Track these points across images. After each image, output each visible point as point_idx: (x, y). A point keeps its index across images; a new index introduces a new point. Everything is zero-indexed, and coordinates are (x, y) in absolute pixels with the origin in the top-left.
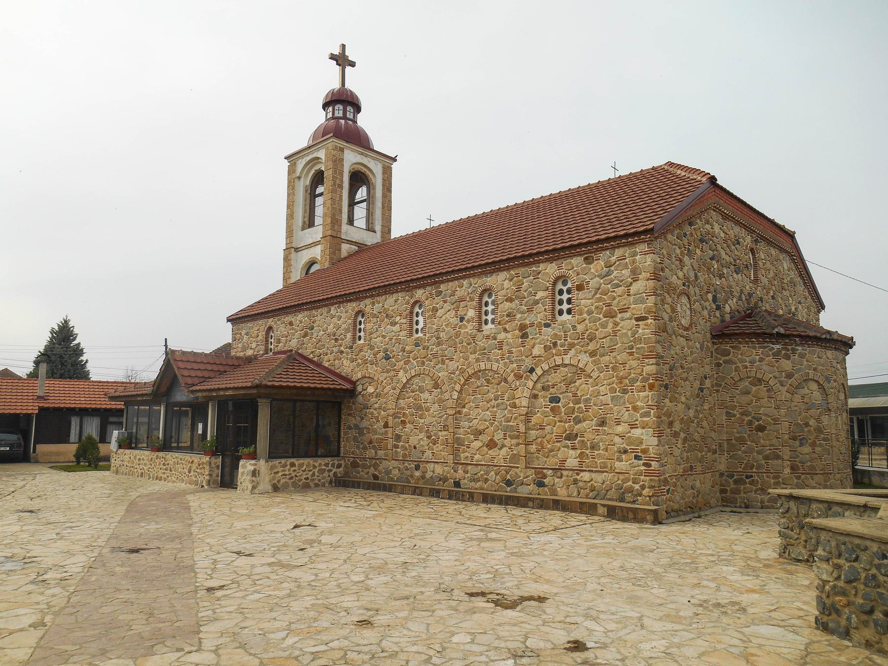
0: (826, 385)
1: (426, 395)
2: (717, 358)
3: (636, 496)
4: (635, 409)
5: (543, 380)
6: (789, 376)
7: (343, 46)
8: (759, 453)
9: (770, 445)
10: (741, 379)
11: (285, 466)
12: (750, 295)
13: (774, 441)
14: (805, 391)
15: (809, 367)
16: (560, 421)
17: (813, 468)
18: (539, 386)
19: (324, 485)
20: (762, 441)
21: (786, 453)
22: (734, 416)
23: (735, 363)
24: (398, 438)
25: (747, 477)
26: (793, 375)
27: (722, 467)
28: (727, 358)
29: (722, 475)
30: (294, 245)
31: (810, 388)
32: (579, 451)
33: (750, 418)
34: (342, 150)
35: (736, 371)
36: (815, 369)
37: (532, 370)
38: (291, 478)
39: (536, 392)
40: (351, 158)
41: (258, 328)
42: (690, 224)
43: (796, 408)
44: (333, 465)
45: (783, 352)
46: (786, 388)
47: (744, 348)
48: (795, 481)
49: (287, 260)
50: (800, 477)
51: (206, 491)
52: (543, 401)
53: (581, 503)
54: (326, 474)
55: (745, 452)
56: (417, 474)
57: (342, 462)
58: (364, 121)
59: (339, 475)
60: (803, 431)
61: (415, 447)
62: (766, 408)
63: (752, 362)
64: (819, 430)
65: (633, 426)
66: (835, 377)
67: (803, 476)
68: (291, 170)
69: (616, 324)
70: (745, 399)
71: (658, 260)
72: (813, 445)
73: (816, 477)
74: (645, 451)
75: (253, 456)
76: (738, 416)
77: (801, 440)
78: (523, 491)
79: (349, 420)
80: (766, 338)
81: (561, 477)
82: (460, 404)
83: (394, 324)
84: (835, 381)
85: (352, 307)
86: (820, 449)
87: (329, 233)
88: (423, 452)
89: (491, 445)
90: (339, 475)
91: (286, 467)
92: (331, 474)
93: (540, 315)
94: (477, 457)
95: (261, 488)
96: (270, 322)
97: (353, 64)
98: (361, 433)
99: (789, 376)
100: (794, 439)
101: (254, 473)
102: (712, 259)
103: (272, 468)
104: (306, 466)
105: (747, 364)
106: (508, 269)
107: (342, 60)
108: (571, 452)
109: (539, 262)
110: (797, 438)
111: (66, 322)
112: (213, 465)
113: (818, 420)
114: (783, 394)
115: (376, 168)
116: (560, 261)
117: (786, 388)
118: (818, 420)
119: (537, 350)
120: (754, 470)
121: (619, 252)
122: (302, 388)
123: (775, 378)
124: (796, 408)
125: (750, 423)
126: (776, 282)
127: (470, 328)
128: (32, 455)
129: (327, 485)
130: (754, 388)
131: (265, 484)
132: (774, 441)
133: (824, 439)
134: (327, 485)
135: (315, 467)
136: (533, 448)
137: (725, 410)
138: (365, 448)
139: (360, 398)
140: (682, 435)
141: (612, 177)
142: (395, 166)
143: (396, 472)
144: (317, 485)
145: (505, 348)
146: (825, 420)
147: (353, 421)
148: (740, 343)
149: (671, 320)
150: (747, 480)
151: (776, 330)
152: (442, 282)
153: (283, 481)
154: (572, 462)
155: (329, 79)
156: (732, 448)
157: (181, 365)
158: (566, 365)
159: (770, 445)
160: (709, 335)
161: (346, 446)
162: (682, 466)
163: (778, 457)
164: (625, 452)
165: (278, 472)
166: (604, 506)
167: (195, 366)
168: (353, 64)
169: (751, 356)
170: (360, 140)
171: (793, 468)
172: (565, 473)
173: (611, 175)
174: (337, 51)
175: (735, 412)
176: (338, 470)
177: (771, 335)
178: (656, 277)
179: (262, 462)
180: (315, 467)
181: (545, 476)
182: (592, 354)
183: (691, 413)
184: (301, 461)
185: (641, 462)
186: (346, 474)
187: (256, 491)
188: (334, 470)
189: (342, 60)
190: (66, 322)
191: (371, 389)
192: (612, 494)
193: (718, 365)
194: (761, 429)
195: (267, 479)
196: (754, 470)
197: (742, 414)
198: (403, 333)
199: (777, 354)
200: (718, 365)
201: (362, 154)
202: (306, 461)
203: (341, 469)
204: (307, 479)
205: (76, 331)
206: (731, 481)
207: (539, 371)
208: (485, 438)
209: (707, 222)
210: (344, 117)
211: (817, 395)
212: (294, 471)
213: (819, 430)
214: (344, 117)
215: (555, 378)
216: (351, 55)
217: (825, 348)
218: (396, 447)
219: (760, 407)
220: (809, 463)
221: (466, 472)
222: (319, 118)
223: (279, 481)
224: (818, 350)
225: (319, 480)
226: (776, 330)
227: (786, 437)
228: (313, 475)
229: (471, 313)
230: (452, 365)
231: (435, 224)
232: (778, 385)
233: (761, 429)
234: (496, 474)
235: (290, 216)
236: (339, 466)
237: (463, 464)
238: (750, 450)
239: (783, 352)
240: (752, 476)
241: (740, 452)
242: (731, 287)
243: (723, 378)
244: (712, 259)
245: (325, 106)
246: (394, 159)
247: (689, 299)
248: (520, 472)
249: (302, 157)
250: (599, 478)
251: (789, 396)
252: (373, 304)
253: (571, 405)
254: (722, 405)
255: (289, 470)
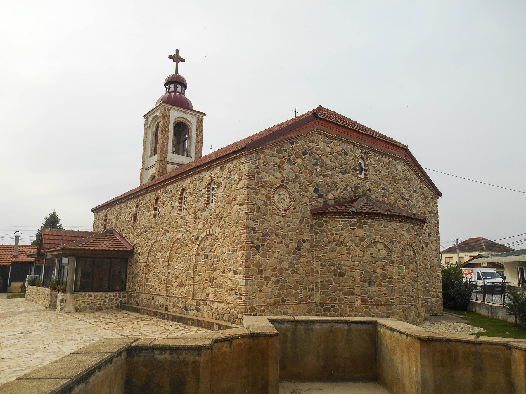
0: (390, 245)
1: (158, 254)
2: (316, 229)
3: (235, 318)
4: (237, 262)
5: (202, 244)
6: (362, 239)
7: (177, 51)
8: (340, 290)
9: (348, 286)
10: (329, 242)
11: (85, 296)
12: (357, 187)
13: (351, 283)
14: (374, 249)
15: (377, 234)
16: (208, 270)
17: (379, 301)
18: (200, 248)
19: (112, 308)
20: (342, 283)
21: (358, 291)
22: (325, 266)
23: (326, 232)
24: (147, 280)
25: (332, 307)
26: (364, 239)
27: (317, 300)
28: (321, 228)
29: (317, 305)
30: (146, 166)
31: (378, 247)
32: (214, 289)
33: (335, 268)
34: (169, 110)
35: (326, 237)
36: (381, 235)
37: (197, 238)
38: (89, 304)
39: (199, 251)
40: (175, 114)
41: (102, 214)
42: (292, 143)
43: (366, 261)
44: (119, 296)
45: (358, 224)
46: (359, 248)
47: (332, 222)
48: (364, 310)
49: (142, 175)
50: (368, 307)
51: (48, 310)
52: (201, 258)
53: (208, 322)
54: (114, 302)
55: (331, 290)
56: (153, 302)
57: (126, 294)
58: (188, 94)
59: (124, 302)
60: (371, 276)
61: (153, 286)
62: (345, 262)
63: (337, 231)
64: (384, 276)
65: (236, 273)
66: (399, 240)
67: (370, 307)
68: (146, 124)
69: (231, 208)
70: (332, 255)
71: (253, 167)
72: (379, 285)
73: (380, 307)
74: (239, 289)
75: (64, 291)
76: (328, 266)
77: (369, 282)
78: (192, 314)
79: (131, 269)
80: (345, 215)
81: (206, 305)
82: (170, 259)
83: (149, 211)
84: (399, 243)
85: (135, 201)
86: (385, 289)
87: (159, 158)
88: (156, 289)
89: (181, 285)
90: (124, 302)
91: (85, 297)
92: (118, 301)
93: (201, 204)
94: (176, 292)
95: (66, 309)
96: (106, 211)
97: (183, 60)
98: (135, 278)
99: (362, 239)
100: (365, 281)
101: (62, 301)
102: (316, 164)
103: (75, 298)
104: (99, 297)
105: (334, 232)
106: (191, 176)
107: (177, 58)
108: (212, 289)
109: (202, 171)
110: (367, 280)
111: (54, 213)
112: (53, 296)
113: (384, 269)
114: (358, 251)
115: (192, 120)
116: (211, 170)
117: (359, 248)
118: (384, 269)
119: (200, 226)
120: (337, 302)
121: (234, 162)
122: (94, 250)
123: (352, 241)
124: (366, 261)
125: (335, 271)
126: (387, 179)
128: (8, 288)
129: (115, 308)
130: (338, 248)
131: (70, 307)
132: (351, 283)
133: (388, 282)
134: (115, 308)
135: (106, 297)
136: (196, 287)
137: (320, 263)
138: (135, 286)
139: (135, 255)
140: (274, 279)
141: (294, 117)
142: (205, 118)
143: (145, 301)
144: (107, 308)
145: (188, 224)
146: (389, 269)
147: (132, 269)
148: (329, 218)
149: (265, 204)
150: (332, 309)
151: (351, 209)
152: (167, 185)
153: (82, 306)
154: (211, 297)
155: (169, 69)
156: (323, 287)
157: (47, 237)
158: (211, 235)
159: (348, 286)
160: (309, 214)
161: (129, 285)
162: (273, 299)
163: (353, 294)
164: (232, 290)
165: (79, 300)
166: (217, 324)
167: (56, 238)
168: (183, 60)
169: (336, 227)
170: (185, 105)
171: (363, 301)
172: (208, 303)
173: (293, 116)
174: (173, 53)
175: (326, 264)
176: (123, 299)
177: (349, 213)
178: (250, 177)
179: (68, 294)
180: (106, 297)
181: (200, 305)
182: (221, 227)
183: (285, 265)
184: (96, 294)
185: (238, 296)
186: (127, 302)
187: (63, 311)
188: (121, 299)
189: (177, 58)
190: (54, 213)
191: (139, 251)
192: (226, 317)
193: (316, 233)
194: (342, 275)
195: (71, 304)
196: (337, 302)
197: (330, 265)
198: (152, 217)
199: (354, 225)
200: (316, 233)
202: (100, 294)
203: (125, 299)
204: (100, 304)
205: (59, 218)
206: (322, 309)
207: (200, 239)
208: (179, 280)
209: (312, 141)
210: (175, 91)
211: (383, 253)
212: (91, 299)
213: (384, 276)
214: (175, 91)
215: (206, 243)
216: (182, 55)
217: (391, 221)
218: (146, 285)
219: (342, 260)
220: (376, 298)
221: (171, 301)
222: (163, 91)
223: (80, 306)
224: (384, 222)
225: (109, 305)
226: (351, 209)
227: (359, 280)
228: (105, 302)
229: (177, 203)
230: (168, 235)
231: (213, 151)
232: (354, 245)
233: (342, 275)
234: (182, 303)
235: (144, 150)
236: (124, 297)
237: (170, 296)
238: (335, 289)
239: (358, 224)
240: (334, 306)
241: (328, 290)
242: (335, 182)
243: (319, 242)
244: (316, 164)
245: (166, 85)
246: (205, 114)
247: (287, 191)
248: (191, 303)
249: (150, 116)
250: (221, 306)
251: (361, 253)
252: (142, 199)
253: (212, 260)
254: (319, 259)
255: (87, 299)
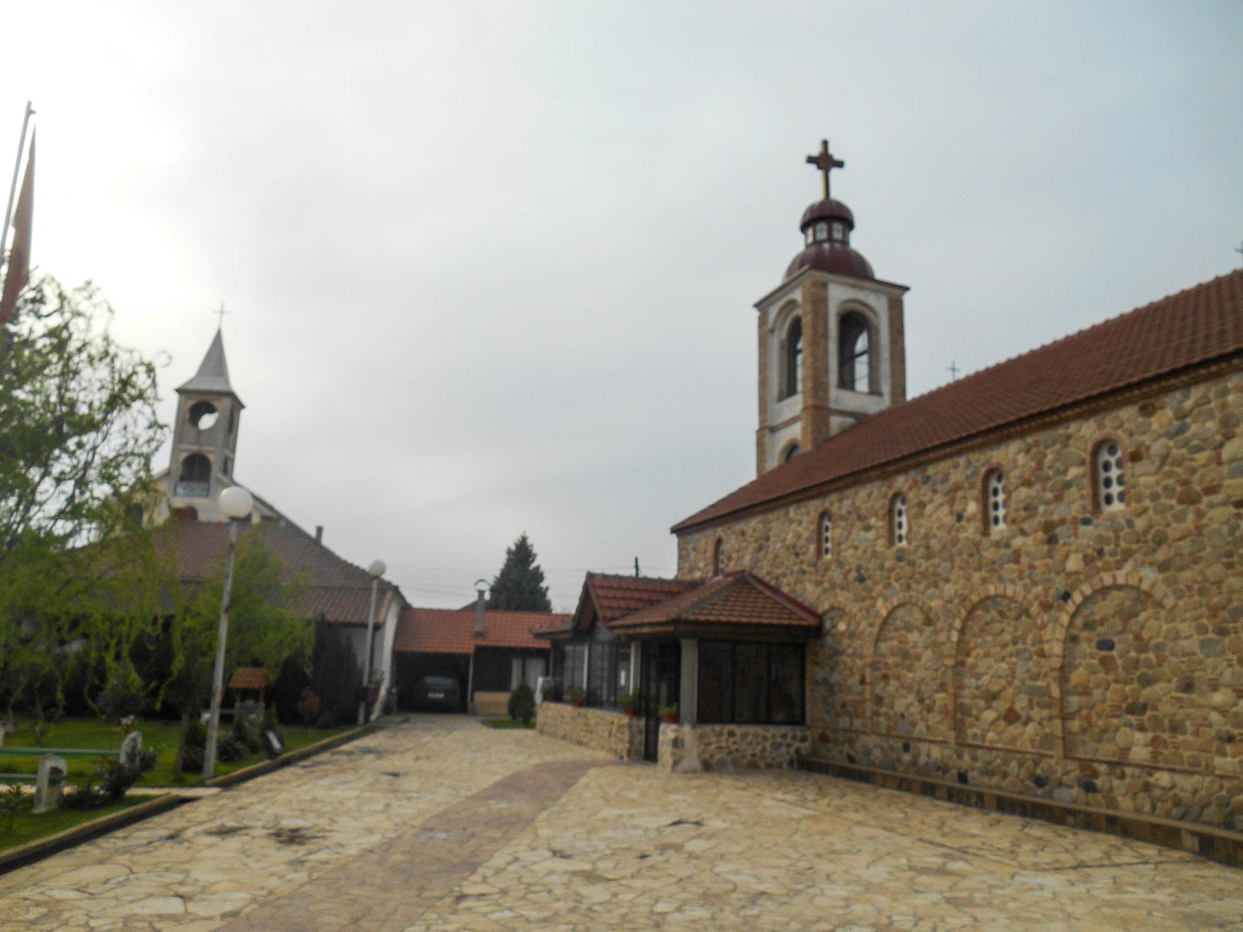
1: (914, 637)
5: (1085, 612)
7: (825, 144)
11: (720, 734)
16: (1116, 682)
18: (1079, 622)
19: (780, 766)
24: (879, 700)
30: (769, 423)
32: (1150, 735)
34: (824, 285)
37: (1066, 596)
39: (1075, 632)
40: (839, 294)
41: (705, 540)
44: (794, 738)
49: (760, 445)
52: (1086, 647)
54: (783, 750)
56: (907, 757)
58: (858, 242)
59: (804, 752)
61: (903, 716)
68: (762, 322)
69: (1200, 514)
75: (675, 719)
79: (815, 672)
82: (963, 649)
83: (868, 528)
85: (815, 506)
87: (810, 402)
88: (914, 724)
89: (1011, 716)
91: (721, 736)
92: (792, 750)
93: (1075, 503)
95: (685, 764)
96: (720, 531)
97: (840, 164)
101: (676, 743)
103: (701, 737)
106: (1021, 435)
107: (825, 162)
108: (1139, 736)
109: (1068, 420)
111: (524, 539)
112: (634, 729)
115: (879, 304)
116: (1100, 416)
119: (1073, 564)
121: (1196, 393)
127: (971, 531)
128: (470, 705)
129: (785, 766)
131: (691, 759)
135: (765, 738)
136: (1075, 725)
138: (837, 715)
139: (829, 640)
142: (907, 298)
143: (877, 753)
144: (769, 766)
152: (929, 462)
153: (717, 757)
154: (1140, 753)
155: (808, 189)
157: (601, 592)
161: (813, 710)
166: (1193, 833)
167: (619, 594)
168: (840, 164)
170: (855, 268)
172: (1129, 771)
174: (816, 151)
179: (687, 730)
181: (1096, 774)
182: (1163, 567)
184: (744, 729)
186: (814, 752)
187: (679, 768)
188: (796, 745)
189: (825, 162)
190: (524, 539)
191: (842, 627)
192: (1211, 812)
195: (695, 753)
198: (881, 542)
201: (854, 286)
203: (807, 745)
204: (754, 755)
205: (535, 550)
207: (1077, 597)
208: (1001, 705)
210: (830, 239)
214: (830, 239)
215: (1104, 608)
216: (836, 152)
218: (877, 714)
221: (975, 759)
222: (797, 244)
223: (712, 756)
225: (773, 759)
228: (764, 750)
229: (972, 508)
230: (949, 589)
231: (960, 376)
234: (1021, 765)
235: (763, 385)
236: (804, 739)
245: (804, 227)
246: (906, 289)
248: (1055, 764)
249: (774, 303)
250: (1186, 784)
252: (840, 500)
253: (1133, 654)
